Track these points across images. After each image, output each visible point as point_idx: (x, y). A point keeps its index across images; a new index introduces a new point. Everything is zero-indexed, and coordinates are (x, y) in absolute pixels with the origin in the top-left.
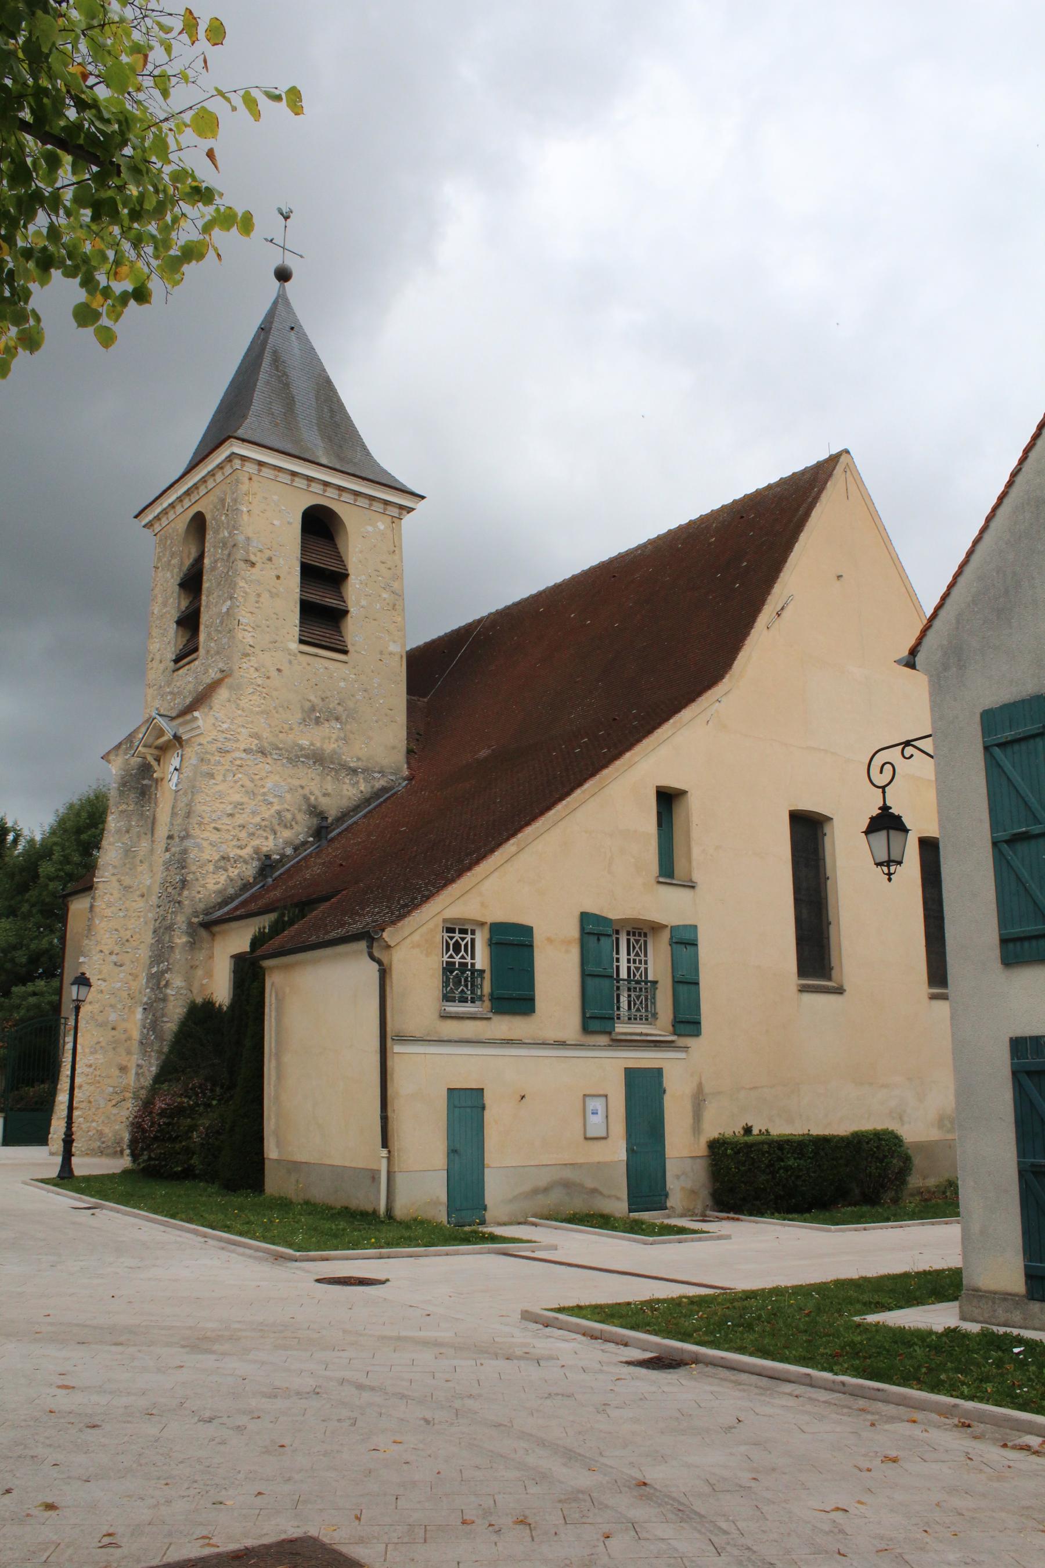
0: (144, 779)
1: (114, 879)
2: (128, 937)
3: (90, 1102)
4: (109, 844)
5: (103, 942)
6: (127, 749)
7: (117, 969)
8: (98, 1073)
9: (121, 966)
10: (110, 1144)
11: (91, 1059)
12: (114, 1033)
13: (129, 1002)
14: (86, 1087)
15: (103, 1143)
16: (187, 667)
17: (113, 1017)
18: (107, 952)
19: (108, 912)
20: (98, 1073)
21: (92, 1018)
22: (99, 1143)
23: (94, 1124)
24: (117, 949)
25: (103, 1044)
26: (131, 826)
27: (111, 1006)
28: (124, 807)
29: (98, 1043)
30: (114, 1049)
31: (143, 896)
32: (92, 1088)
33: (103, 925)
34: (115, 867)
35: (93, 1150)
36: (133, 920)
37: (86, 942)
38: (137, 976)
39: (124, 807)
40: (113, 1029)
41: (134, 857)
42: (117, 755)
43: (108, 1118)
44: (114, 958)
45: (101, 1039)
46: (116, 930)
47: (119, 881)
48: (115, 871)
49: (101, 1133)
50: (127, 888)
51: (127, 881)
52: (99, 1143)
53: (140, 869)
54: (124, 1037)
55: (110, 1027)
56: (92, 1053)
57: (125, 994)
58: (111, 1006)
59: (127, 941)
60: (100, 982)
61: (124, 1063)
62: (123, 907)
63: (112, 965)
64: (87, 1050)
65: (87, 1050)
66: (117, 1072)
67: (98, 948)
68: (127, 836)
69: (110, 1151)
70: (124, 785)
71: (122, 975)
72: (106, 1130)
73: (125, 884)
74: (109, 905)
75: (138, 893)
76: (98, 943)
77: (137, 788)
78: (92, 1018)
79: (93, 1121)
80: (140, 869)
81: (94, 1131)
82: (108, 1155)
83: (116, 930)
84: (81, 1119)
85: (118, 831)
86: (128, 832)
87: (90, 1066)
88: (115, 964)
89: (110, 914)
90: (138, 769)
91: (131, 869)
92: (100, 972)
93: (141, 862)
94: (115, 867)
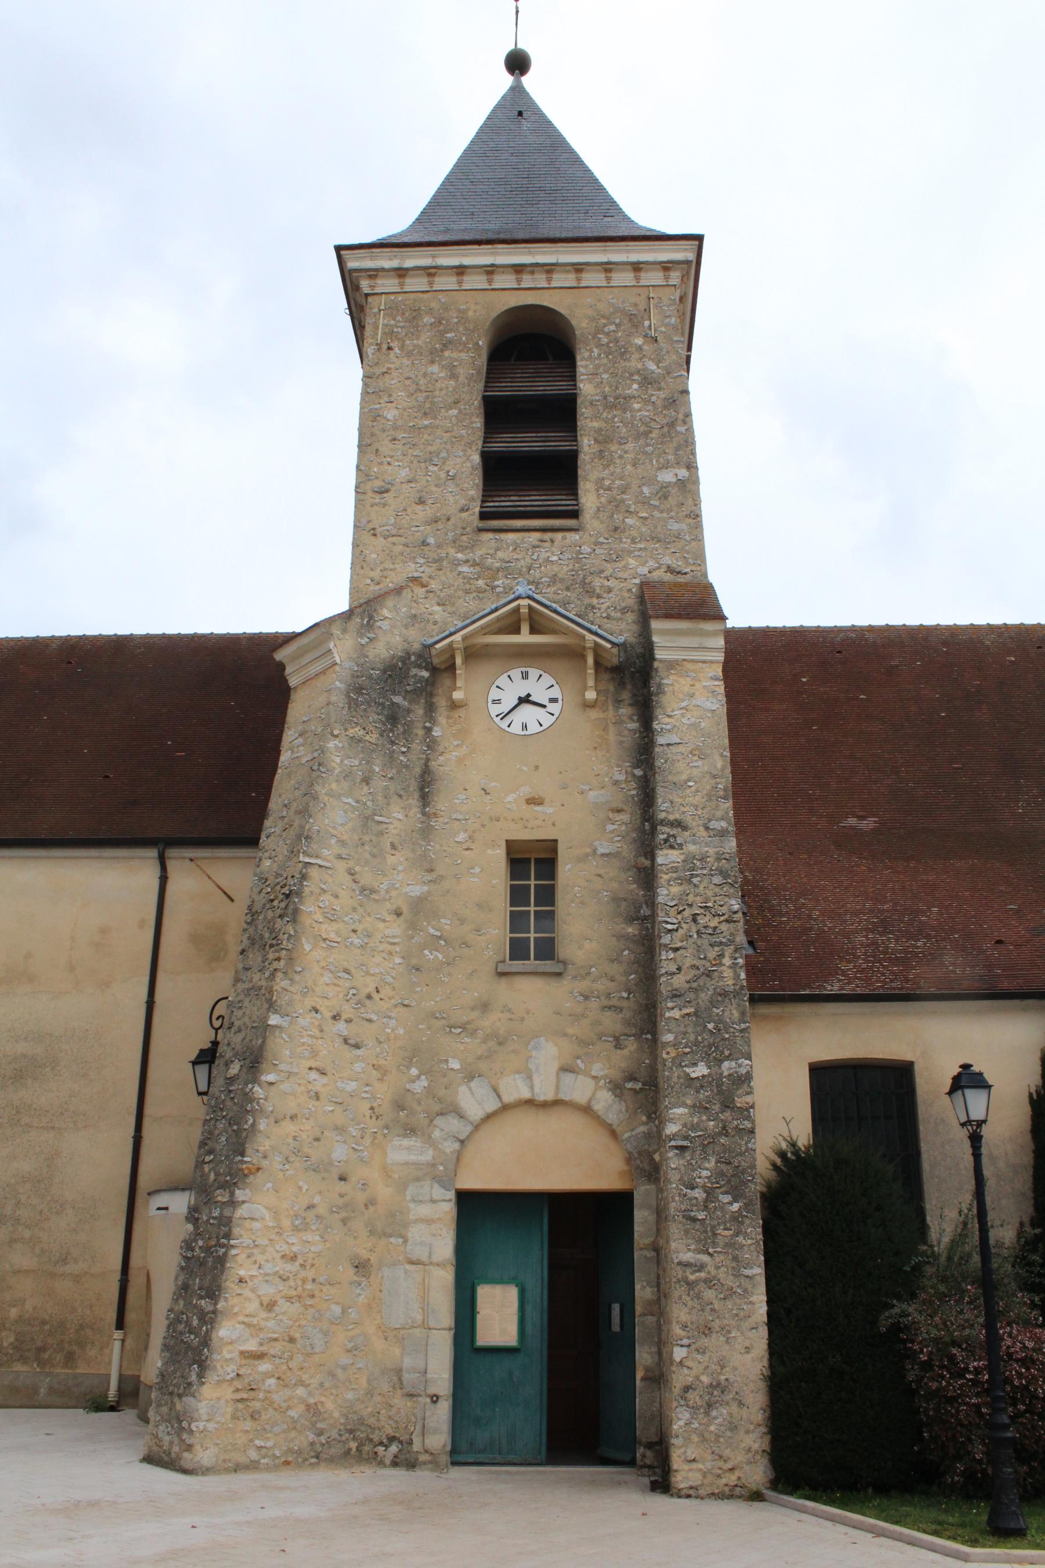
0: (394, 693)
1: (341, 866)
2: (371, 989)
3: (292, 1340)
4: (330, 794)
5: (318, 990)
6: (362, 624)
7: (349, 1053)
8: (310, 1274)
9: (357, 1046)
10: (334, 1434)
11: (295, 1243)
12: (341, 1187)
13: (373, 1125)
14: (283, 1305)
15: (320, 1433)
16: (537, 535)
17: (340, 1152)
18: (328, 1015)
19: (329, 930)
20: (310, 1274)
21: (297, 1151)
22: (311, 1437)
23: (300, 1391)
24: (348, 1011)
25: (321, 1210)
26: (372, 772)
27: (336, 1128)
28: (357, 731)
29: (310, 1207)
30: (344, 1221)
31: (399, 914)
32: (295, 1308)
33: (318, 954)
34: (342, 843)
35: (299, 1452)
36: (378, 959)
37: (285, 984)
38: (385, 1073)
39: (357, 731)
40: (342, 1178)
41: (381, 834)
42: (344, 631)
43: (333, 1375)
44: (341, 1026)
45: (317, 1200)
46: (347, 971)
47: (351, 873)
48: (344, 852)
49: (313, 1411)
50: (367, 891)
51: (367, 878)
52: (311, 1437)
53: (391, 860)
54: (361, 1197)
55: (335, 1174)
56: (296, 1229)
57: (365, 1107)
58: (336, 1128)
59: (369, 997)
60: (314, 1075)
61: (365, 1254)
62: (360, 928)
63: (338, 1043)
64: (286, 1223)
65: (286, 1223)
66: (349, 1273)
67: (309, 1002)
68: (366, 788)
69: (336, 1450)
70: (359, 690)
71: (358, 1067)
72: (329, 1405)
73: (363, 882)
74: (331, 917)
75: (388, 905)
76: (307, 991)
77: (383, 704)
78: (297, 1151)
79: (302, 1383)
80: (391, 860)
81: (302, 1407)
82: (332, 1460)
83: (347, 971)
84: (272, 1381)
85: (347, 775)
86: (366, 781)
87: (294, 1258)
88: (346, 1041)
89: (332, 936)
90: (384, 671)
91: (374, 856)
92: (314, 1054)
93: (393, 846)
94: (342, 843)
